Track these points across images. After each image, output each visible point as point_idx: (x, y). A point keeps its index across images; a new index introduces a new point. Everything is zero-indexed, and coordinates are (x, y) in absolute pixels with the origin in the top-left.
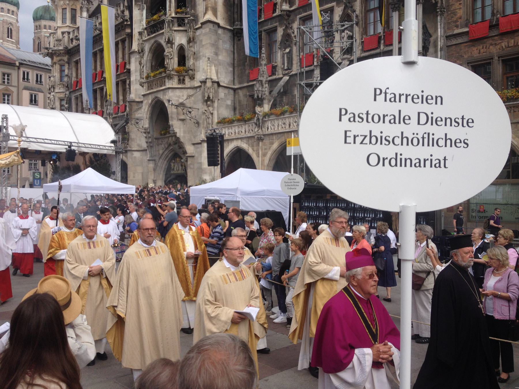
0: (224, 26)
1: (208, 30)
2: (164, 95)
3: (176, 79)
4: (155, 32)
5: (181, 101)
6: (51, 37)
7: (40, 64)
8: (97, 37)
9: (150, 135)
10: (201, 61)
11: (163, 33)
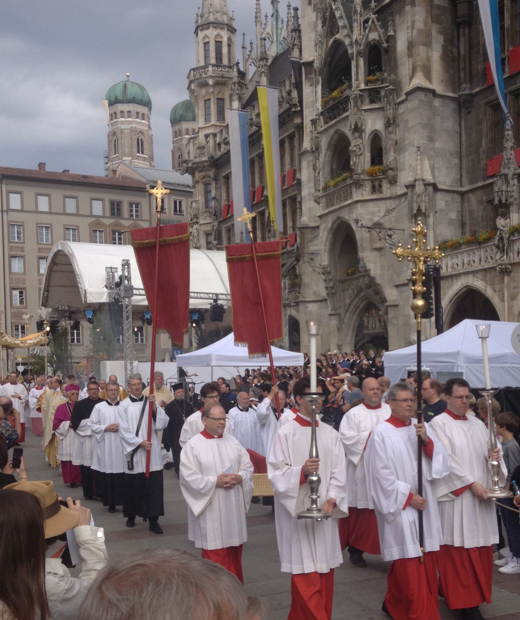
0: (443, 93)
1: (416, 102)
2: (351, 212)
3: (368, 187)
5: (376, 219)
6: (191, 144)
7: (178, 185)
8: (254, 137)
9: (330, 277)
10: (406, 153)
11: (347, 116)
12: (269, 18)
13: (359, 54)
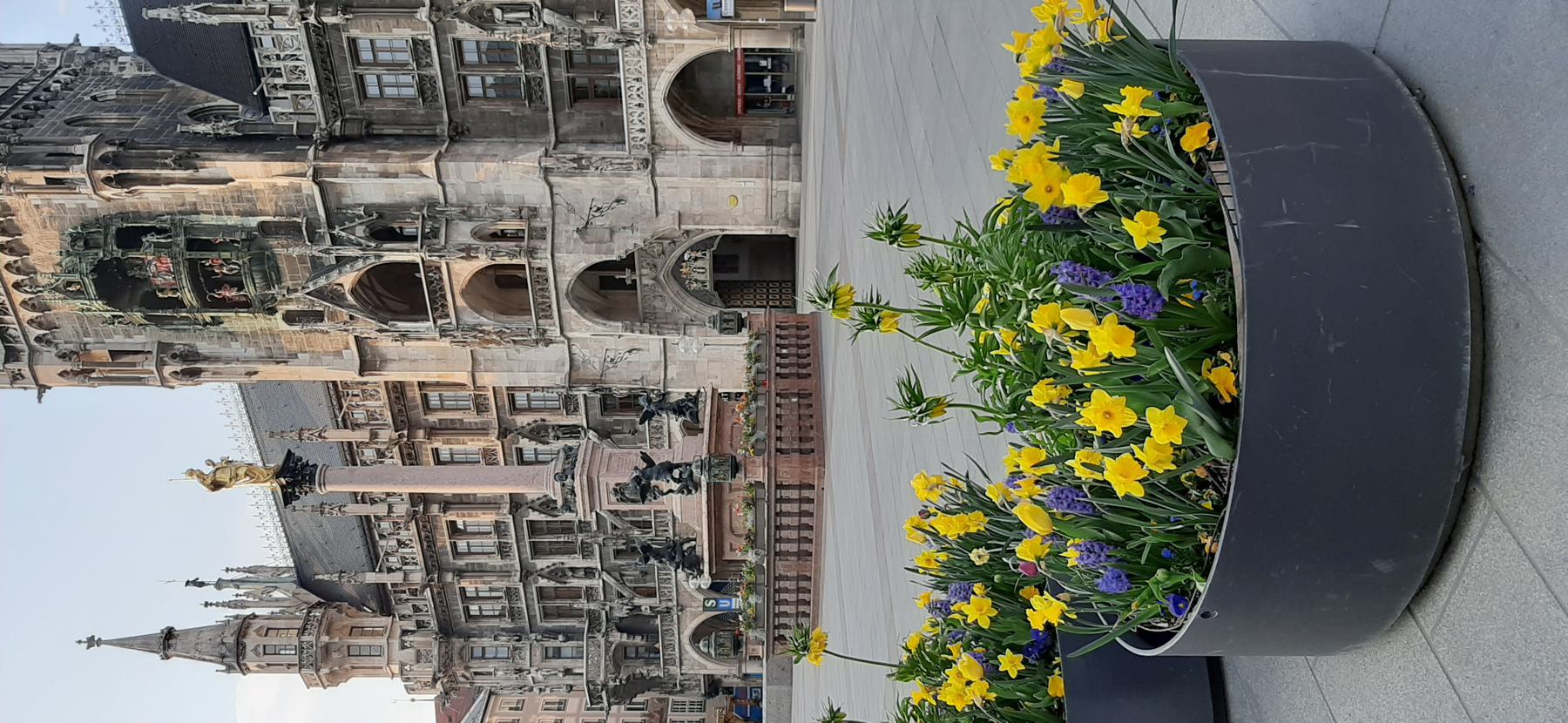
1: (452, 164)
4: (444, 297)
12: (241, 592)
13: (376, 249)
